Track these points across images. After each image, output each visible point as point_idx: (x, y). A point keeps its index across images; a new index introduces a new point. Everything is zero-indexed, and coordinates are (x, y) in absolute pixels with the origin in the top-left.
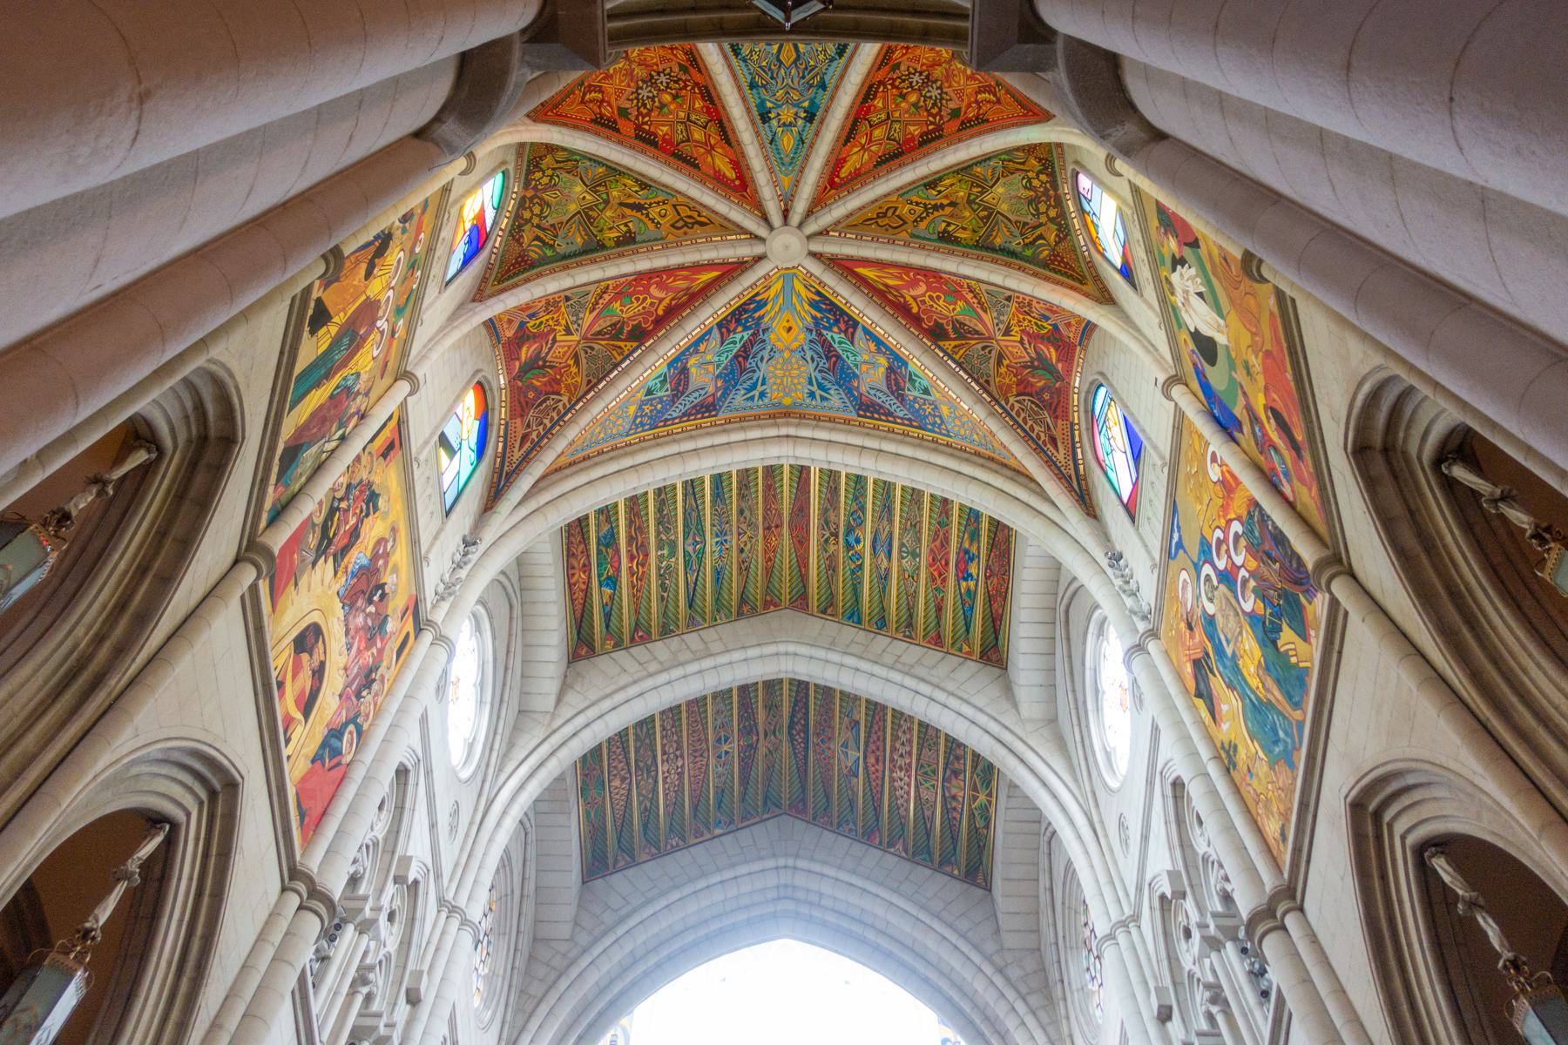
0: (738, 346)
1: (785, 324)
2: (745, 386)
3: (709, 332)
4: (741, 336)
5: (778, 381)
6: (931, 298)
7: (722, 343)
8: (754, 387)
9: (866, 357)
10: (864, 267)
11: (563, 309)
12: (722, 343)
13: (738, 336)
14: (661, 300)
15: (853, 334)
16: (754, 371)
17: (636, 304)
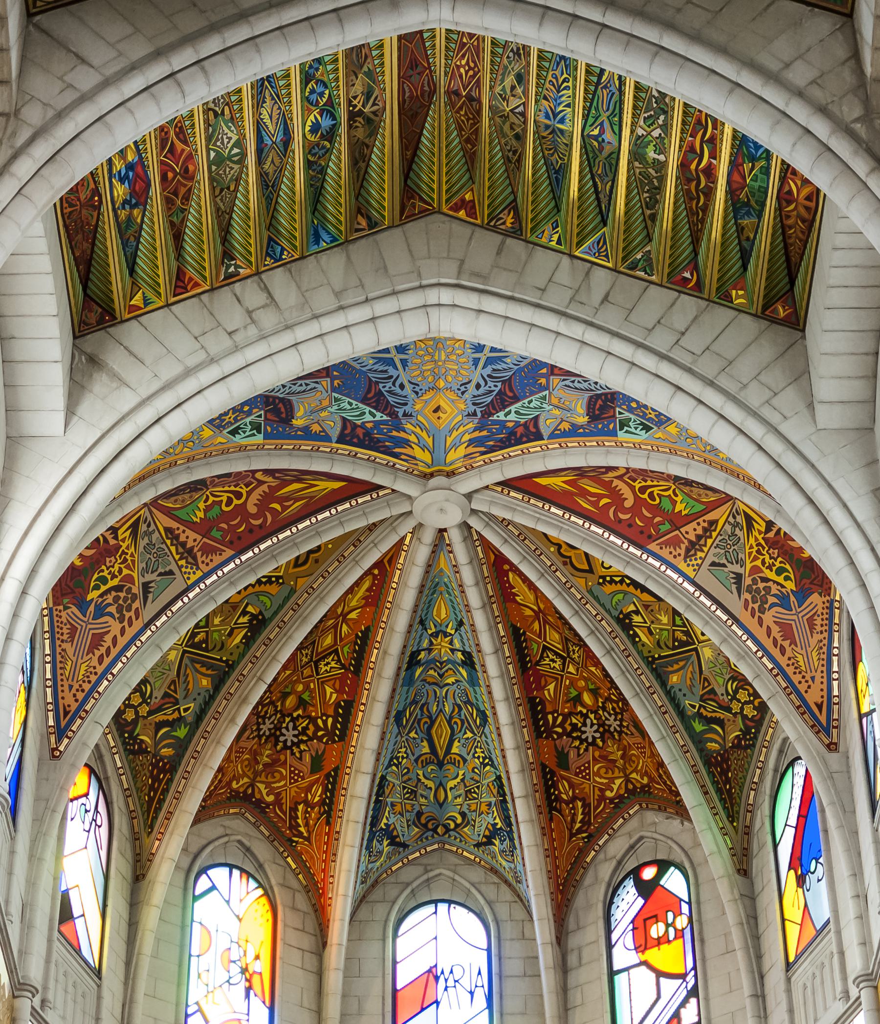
0: (513, 408)
1: (441, 415)
2: (505, 366)
3: (552, 436)
4: (510, 416)
5: (454, 357)
6: (238, 495)
7: (536, 418)
8: (489, 361)
9: (324, 414)
10: (334, 491)
11: (749, 566)
12: (536, 418)
13: (512, 417)
14: (620, 478)
15: (344, 427)
16: (489, 376)
17: (656, 491)
